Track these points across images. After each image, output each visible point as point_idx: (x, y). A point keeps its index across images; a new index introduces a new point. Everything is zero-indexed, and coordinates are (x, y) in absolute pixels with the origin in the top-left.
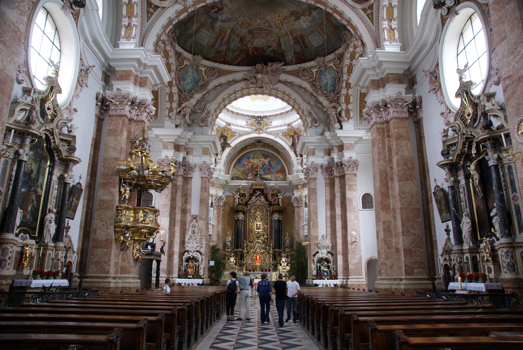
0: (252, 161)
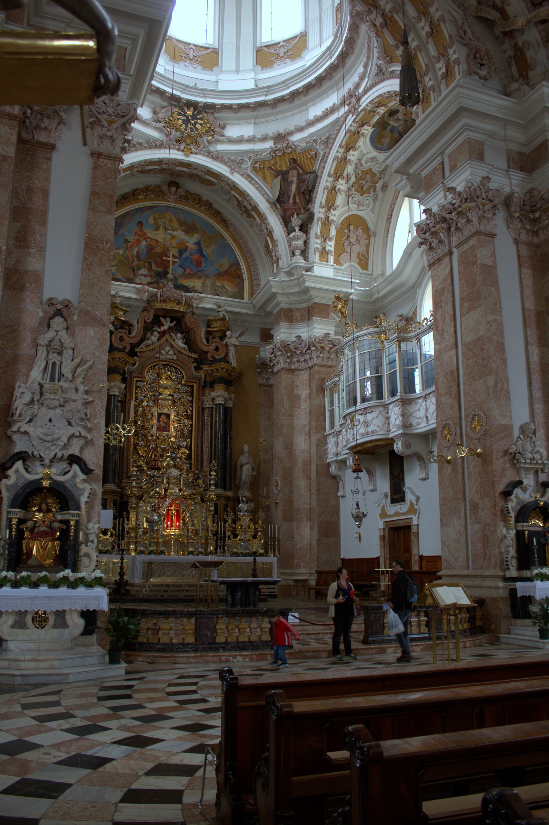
0: (150, 233)
